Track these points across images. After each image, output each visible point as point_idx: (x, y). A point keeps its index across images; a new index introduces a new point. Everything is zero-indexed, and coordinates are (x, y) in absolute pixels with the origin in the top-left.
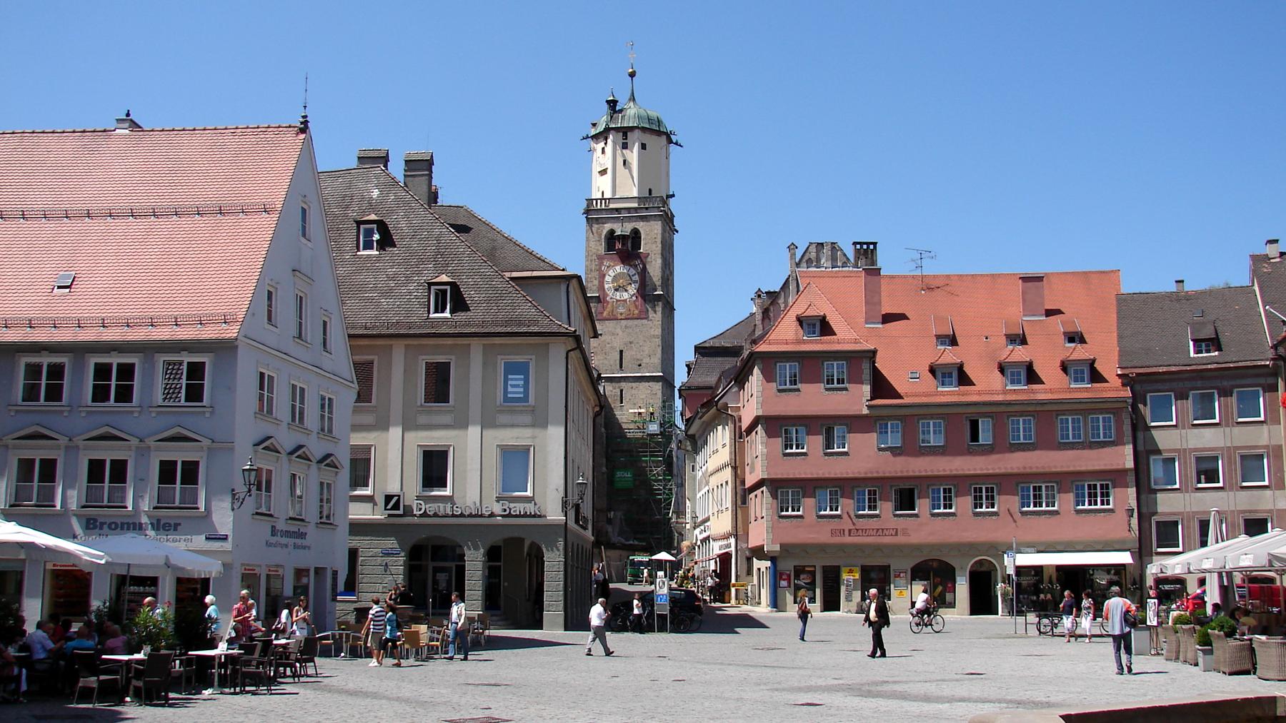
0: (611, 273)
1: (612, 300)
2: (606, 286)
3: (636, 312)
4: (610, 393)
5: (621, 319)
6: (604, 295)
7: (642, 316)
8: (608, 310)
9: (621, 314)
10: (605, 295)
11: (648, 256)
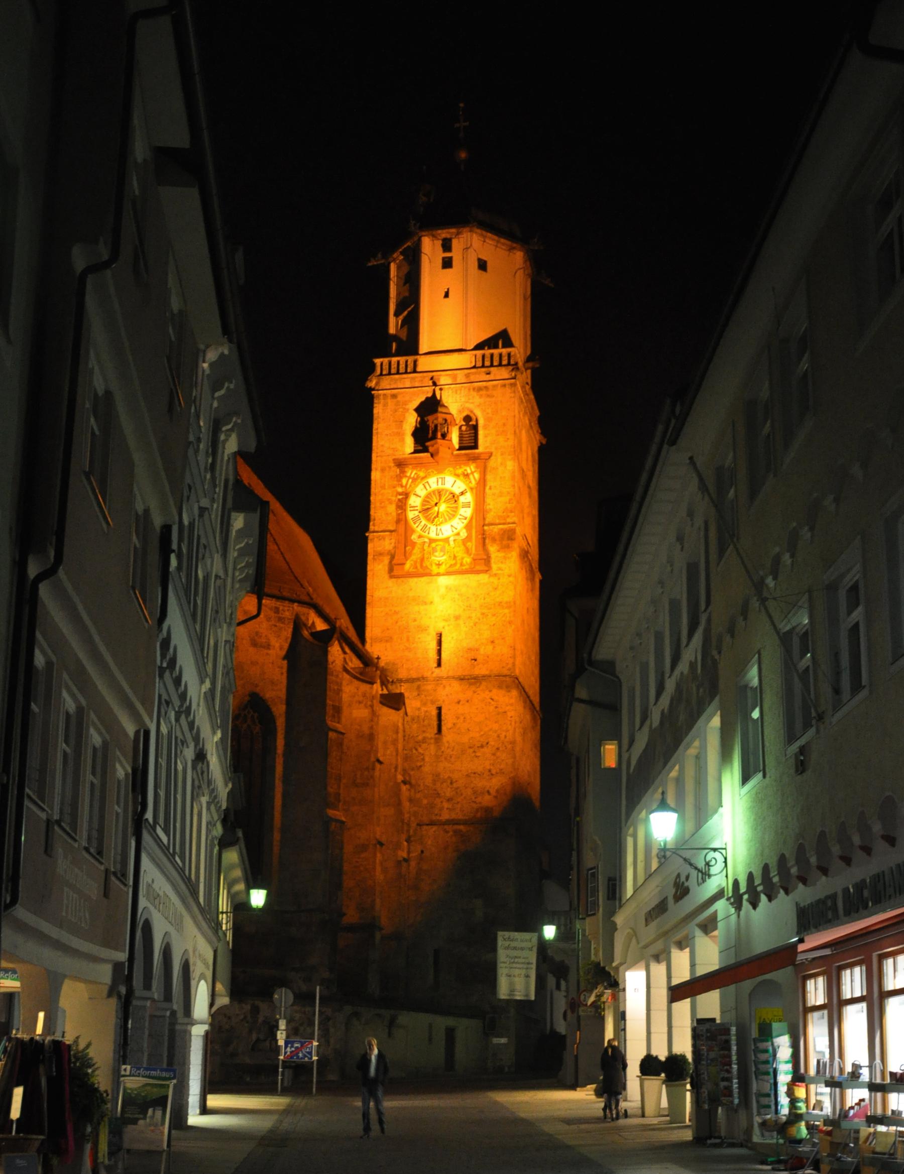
0: (421, 491)
1: (421, 540)
2: (411, 515)
3: (468, 560)
4: (417, 713)
5: (438, 574)
6: (406, 529)
7: (478, 568)
8: (414, 557)
9: (439, 565)
10: (408, 530)
11: (490, 457)
